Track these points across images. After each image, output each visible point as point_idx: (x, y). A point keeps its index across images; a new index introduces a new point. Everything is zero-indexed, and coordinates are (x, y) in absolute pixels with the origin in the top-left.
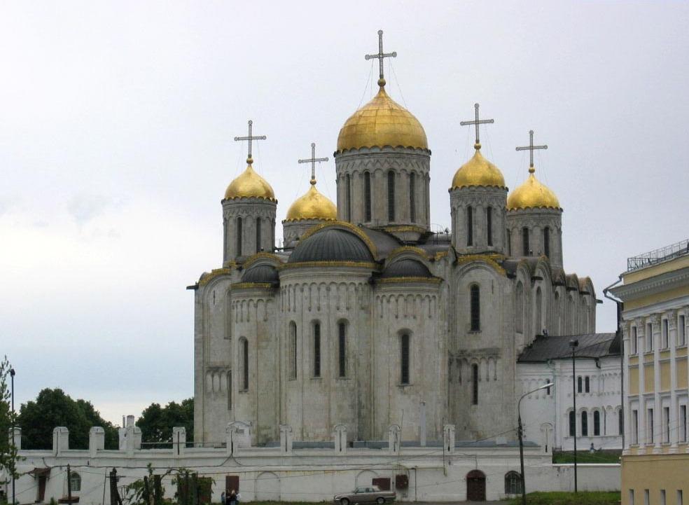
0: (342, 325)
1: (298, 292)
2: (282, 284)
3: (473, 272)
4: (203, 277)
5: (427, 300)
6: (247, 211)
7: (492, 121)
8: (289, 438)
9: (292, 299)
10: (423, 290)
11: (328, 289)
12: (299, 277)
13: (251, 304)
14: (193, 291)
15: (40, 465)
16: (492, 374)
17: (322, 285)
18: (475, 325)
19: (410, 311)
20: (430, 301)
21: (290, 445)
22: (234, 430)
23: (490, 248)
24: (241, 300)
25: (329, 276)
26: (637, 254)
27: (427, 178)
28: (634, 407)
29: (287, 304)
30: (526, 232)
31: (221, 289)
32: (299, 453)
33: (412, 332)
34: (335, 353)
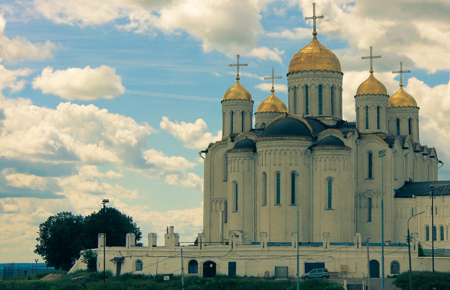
0: (293, 175)
1: (268, 156)
2: (258, 150)
3: (368, 144)
4: (211, 145)
5: (342, 159)
9: (264, 159)
10: (340, 155)
11: (285, 153)
12: (269, 146)
13: (240, 161)
14: (204, 155)
17: (282, 151)
18: (370, 176)
20: (344, 161)
21: (266, 245)
22: (233, 235)
23: (378, 131)
24: (234, 159)
25: (286, 146)
27: (341, 90)
29: (261, 162)
30: (398, 121)
33: (333, 178)
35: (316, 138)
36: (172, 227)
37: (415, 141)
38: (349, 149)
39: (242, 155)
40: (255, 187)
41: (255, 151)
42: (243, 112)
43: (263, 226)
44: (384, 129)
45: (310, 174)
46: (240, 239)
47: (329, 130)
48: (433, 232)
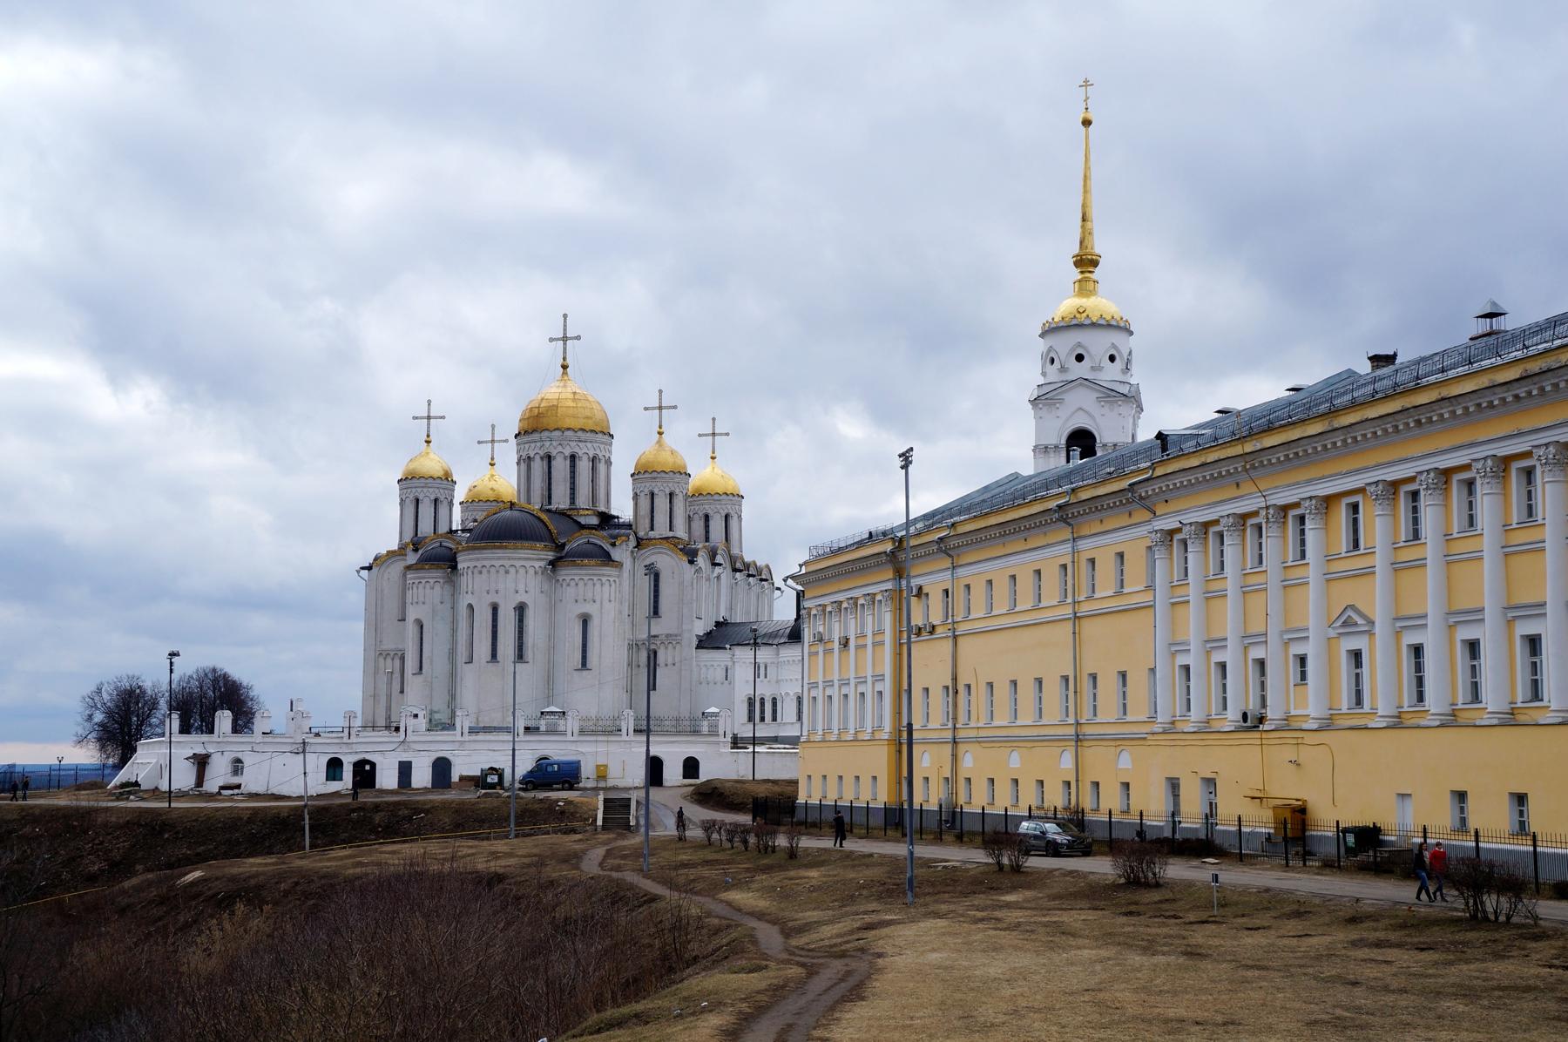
0: (521, 609)
2: (460, 566)
6: (424, 491)
7: (675, 407)
8: (464, 722)
14: (365, 573)
15: (200, 750)
16: (670, 661)
18: (656, 612)
19: (590, 595)
21: (466, 730)
26: (819, 543)
27: (609, 463)
28: (813, 693)
30: (707, 517)
31: (397, 567)
32: (474, 737)
35: (564, 545)
36: (300, 700)
37: (735, 551)
38: (619, 565)
39: (435, 576)
40: (454, 631)
41: (454, 567)
42: (436, 500)
44: (681, 532)
45: (553, 607)
46: (422, 722)
47: (585, 532)
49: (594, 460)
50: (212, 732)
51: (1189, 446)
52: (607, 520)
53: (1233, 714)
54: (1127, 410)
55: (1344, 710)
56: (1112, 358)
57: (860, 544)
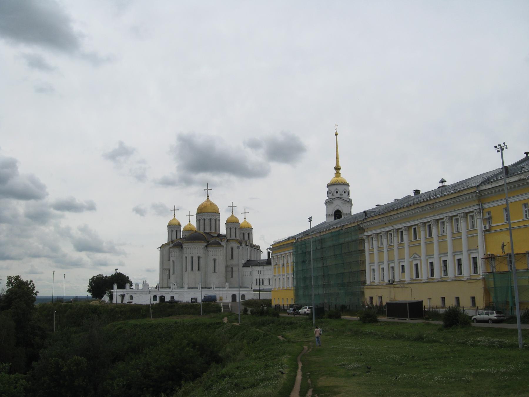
0: (199, 258)
4: (162, 245)
8: (186, 286)
14: (159, 249)
15: (122, 293)
18: (232, 258)
30: (244, 234)
34: (198, 265)
38: (223, 246)
40: (182, 263)
41: (182, 247)
43: (186, 280)
44: (238, 238)
46: (176, 286)
48: (260, 282)
49: (216, 220)
50: (125, 289)
51: (372, 214)
52: (219, 235)
53: (386, 281)
54: (349, 205)
55: (414, 278)
56: (345, 192)
57: (287, 240)
